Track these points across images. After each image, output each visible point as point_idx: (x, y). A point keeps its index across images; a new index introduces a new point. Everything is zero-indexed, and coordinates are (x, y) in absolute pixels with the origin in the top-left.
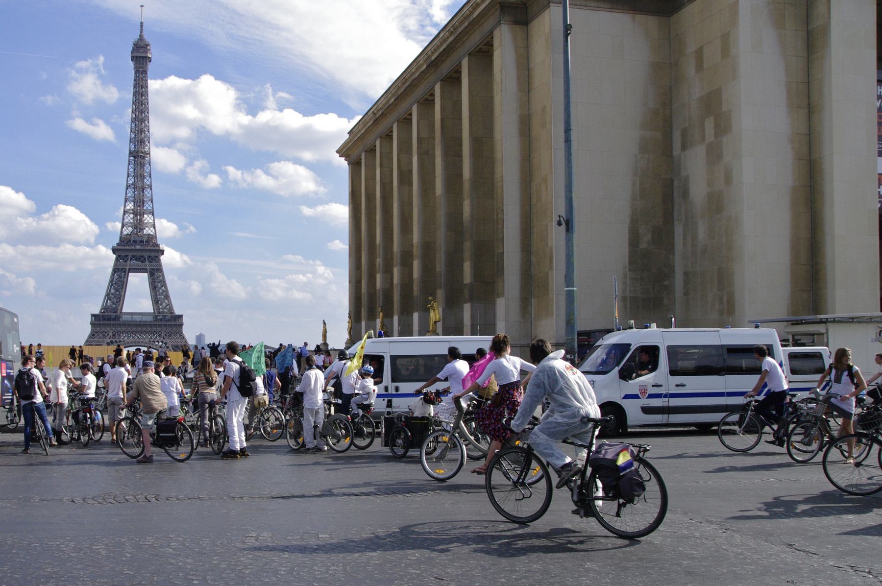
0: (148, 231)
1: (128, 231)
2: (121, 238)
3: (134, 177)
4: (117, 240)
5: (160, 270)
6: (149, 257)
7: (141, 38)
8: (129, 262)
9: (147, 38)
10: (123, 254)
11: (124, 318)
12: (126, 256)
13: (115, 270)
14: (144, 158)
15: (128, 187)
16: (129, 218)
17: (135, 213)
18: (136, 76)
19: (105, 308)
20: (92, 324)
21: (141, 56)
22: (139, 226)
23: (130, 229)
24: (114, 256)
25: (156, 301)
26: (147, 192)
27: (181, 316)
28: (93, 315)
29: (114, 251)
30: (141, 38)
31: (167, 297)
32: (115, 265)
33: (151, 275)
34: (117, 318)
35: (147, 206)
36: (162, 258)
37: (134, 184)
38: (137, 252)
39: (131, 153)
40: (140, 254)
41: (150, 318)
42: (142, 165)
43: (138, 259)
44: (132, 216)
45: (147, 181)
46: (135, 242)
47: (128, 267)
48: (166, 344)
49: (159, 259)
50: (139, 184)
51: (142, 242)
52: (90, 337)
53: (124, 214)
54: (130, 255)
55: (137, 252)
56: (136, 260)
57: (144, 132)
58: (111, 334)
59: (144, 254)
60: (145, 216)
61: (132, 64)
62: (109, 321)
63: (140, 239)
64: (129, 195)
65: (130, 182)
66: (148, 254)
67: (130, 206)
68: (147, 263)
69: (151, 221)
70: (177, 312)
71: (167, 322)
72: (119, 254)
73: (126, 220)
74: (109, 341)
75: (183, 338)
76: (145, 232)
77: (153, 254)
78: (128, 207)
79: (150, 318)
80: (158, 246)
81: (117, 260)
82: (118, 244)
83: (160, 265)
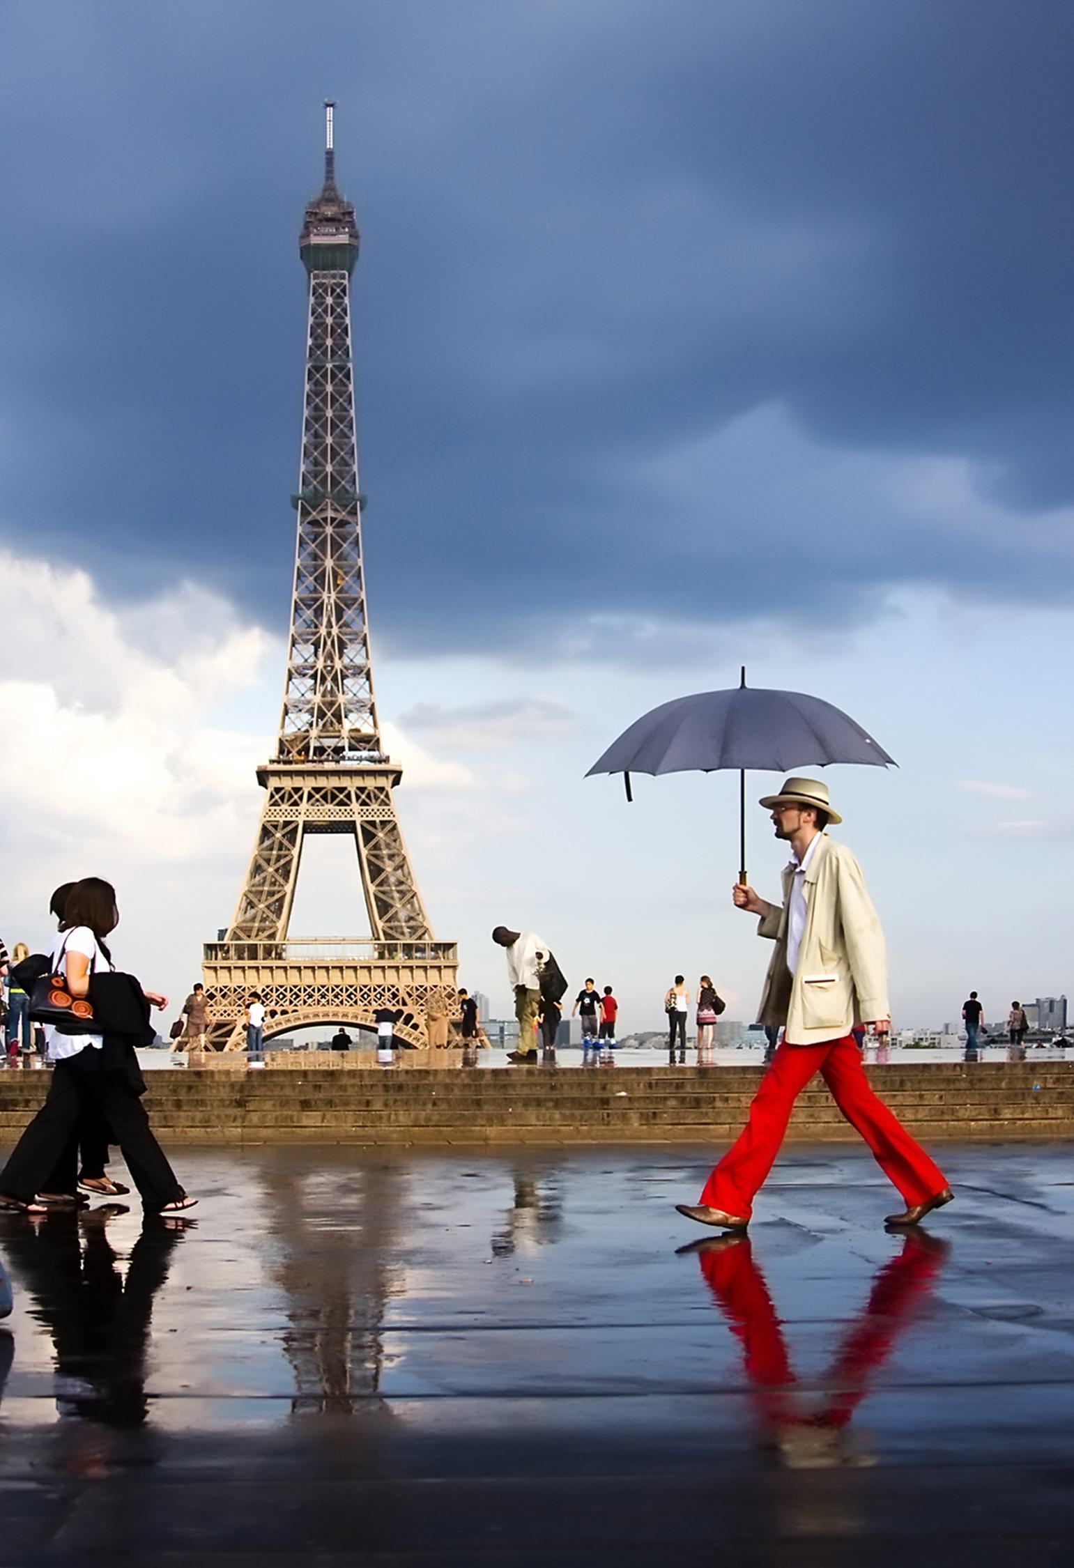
1: (298, 722)
2: (281, 742)
6: (362, 789)
8: (304, 806)
10: (287, 783)
12: (297, 790)
23: (307, 717)
29: (263, 777)
31: (409, 896)
33: (369, 836)
34: (273, 951)
36: (393, 792)
40: (334, 782)
41: (367, 953)
42: (336, 546)
43: (330, 796)
46: (320, 750)
47: (301, 820)
50: (329, 598)
51: (338, 750)
54: (308, 784)
56: (324, 797)
59: (345, 782)
63: (329, 743)
66: (359, 782)
68: (355, 806)
69: (363, 695)
72: (274, 782)
76: (347, 725)
77: (370, 783)
78: (299, 661)
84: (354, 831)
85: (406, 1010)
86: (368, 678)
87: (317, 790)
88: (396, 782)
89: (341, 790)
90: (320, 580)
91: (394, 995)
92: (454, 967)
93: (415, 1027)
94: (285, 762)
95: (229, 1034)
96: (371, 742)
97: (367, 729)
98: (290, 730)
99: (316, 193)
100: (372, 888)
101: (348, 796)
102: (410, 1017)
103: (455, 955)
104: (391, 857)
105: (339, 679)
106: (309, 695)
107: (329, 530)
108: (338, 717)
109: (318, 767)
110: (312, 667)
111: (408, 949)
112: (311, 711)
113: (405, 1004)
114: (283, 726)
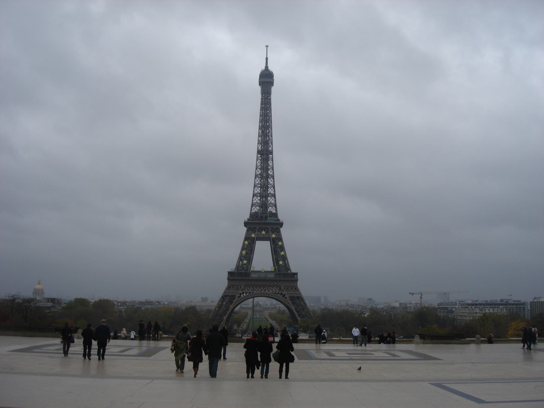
0: (271, 209)
1: (256, 209)
2: (251, 214)
3: (261, 169)
4: (248, 216)
6: (272, 228)
7: (267, 67)
8: (257, 233)
9: (270, 68)
11: (253, 276)
12: (255, 228)
13: (246, 239)
14: (268, 155)
15: (256, 176)
16: (257, 200)
17: (261, 196)
18: (262, 96)
19: (238, 267)
20: (228, 279)
22: (264, 205)
23: (258, 208)
24: (245, 229)
25: (276, 261)
26: (270, 181)
27: (296, 274)
28: (229, 273)
29: (246, 224)
30: (267, 67)
31: (284, 258)
32: (246, 234)
35: (271, 191)
36: (281, 229)
37: (261, 174)
39: (259, 152)
44: (259, 198)
45: (270, 172)
48: (285, 295)
49: (280, 231)
52: (227, 289)
53: (253, 197)
58: (243, 287)
60: (269, 198)
61: (259, 89)
62: (241, 277)
64: (257, 182)
65: (258, 173)
67: (258, 190)
69: (273, 202)
70: (293, 270)
71: (283, 277)
73: (255, 201)
74: (241, 292)
75: (298, 290)
76: (269, 210)
78: (256, 192)
79: (272, 276)
80: (278, 220)
81: (248, 231)
82: (248, 219)
83: (281, 235)
84: (270, 240)
85: (284, 293)
86: (275, 197)
87: (260, 228)
88: (282, 227)
89: (267, 228)
91: (280, 289)
92: (297, 280)
93: (286, 298)
94: (252, 220)
95: (234, 299)
96: (276, 215)
97: (275, 212)
98: (253, 211)
99: (264, 68)
100: (274, 257)
101: (268, 230)
104: (280, 248)
105: (266, 197)
106: (259, 202)
107: (265, 156)
108: (267, 208)
109: (260, 222)
110: (260, 194)
111: (284, 274)
112: (259, 206)
114: (251, 210)
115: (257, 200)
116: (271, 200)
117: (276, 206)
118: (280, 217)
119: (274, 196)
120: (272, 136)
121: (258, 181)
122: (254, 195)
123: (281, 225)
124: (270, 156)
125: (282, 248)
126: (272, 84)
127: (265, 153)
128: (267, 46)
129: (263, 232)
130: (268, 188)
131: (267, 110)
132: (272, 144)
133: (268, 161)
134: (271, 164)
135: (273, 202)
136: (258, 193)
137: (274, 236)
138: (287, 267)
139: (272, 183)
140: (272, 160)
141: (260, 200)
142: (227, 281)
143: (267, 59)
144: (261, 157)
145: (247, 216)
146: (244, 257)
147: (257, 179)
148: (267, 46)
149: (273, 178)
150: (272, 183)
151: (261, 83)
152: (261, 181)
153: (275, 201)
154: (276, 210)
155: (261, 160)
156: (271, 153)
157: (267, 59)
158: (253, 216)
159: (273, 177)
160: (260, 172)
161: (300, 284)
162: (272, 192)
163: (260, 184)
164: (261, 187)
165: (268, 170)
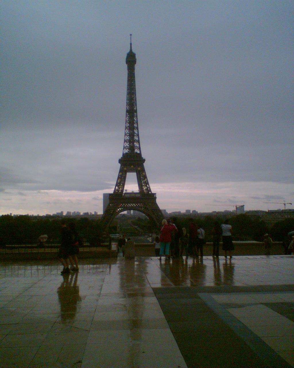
0: (137, 151)
1: (126, 151)
2: (123, 154)
3: (128, 123)
5: (143, 170)
7: (131, 50)
9: (133, 51)
11: (126, 196)
13: (121, 171)
14: (133, 114)
15: (126, 128)
16: (127, 145)
21: (131, 60)
23: (128, 150)
24: (119, 165)
25: (140, 186)
26: (136, 131)
27: (155, 194)
29: (120, 161)
30: (131, 50)
35: (136, 138)
36: (144, 164)
37: (129, 127)
38: (132, 162)
39: (127, 111)
44: (128, 143)
45: (135, 125)
49: (143, 164)
55: (132, 162)
57: (134, 100)
60: (135, 143)
61: (126, 66)
64: (126, 132)
65: (127, 126)
67: (128, 138)
70: (153, 192)
73: (125, 146)
79: (139, 196)
84: (136, 172)
88: (144, 163)
90: (129, 123)
92: (156, 198)
97: (139, 152)
98: (125, 152)
99: (128, 51)
102: (148, 208)
103: (156, 195)
106: (128, 146)
108: (134, 150)
110: (128, 140)
112: (129, 149)
113: (147, 206)
115: (127, 144)
116: (136, 144)
117: (140, 148)
118: (144, 156)
119: (138, 141)
120: (136, 100)
121: (127, 131)
122: (125, 141)
123: (144, 161)
124: (136, 114)
125: (145, 177)
126: (134, 62)
127: (132, 112)
128: (131, 35)
129: (132, 166)
130: (134, 136)
131: (132, 82)
132: (136, 105)
133: (134, 117)
134: (136, 120)
135: (138, 145)
136: (127, 140)
137: (139, 169)
138: (149, 190)
139: (136, 132)
140: (137, 117)
141: (129, 144)
142: (108, 200)
143: (131, 44)
144: (129, 114)
145: (120, 156)
146: (119, 183)
147: (127, 130)
148: (131, 35)
149: (138, 130)
150: (136, 132)
151: (127, 62)
152: (129, 131)
153: (139, 145)
154: (140, 151)
155: (129, 117)
156: (136, 111)
157: (131, 44)
158: (125, 156)
159: (137, 128)
160: (128, 125)
161: (158, 201)
162: (137, 139)
163: (129, 134)
164: (129, 136)
165: (134, 123)
